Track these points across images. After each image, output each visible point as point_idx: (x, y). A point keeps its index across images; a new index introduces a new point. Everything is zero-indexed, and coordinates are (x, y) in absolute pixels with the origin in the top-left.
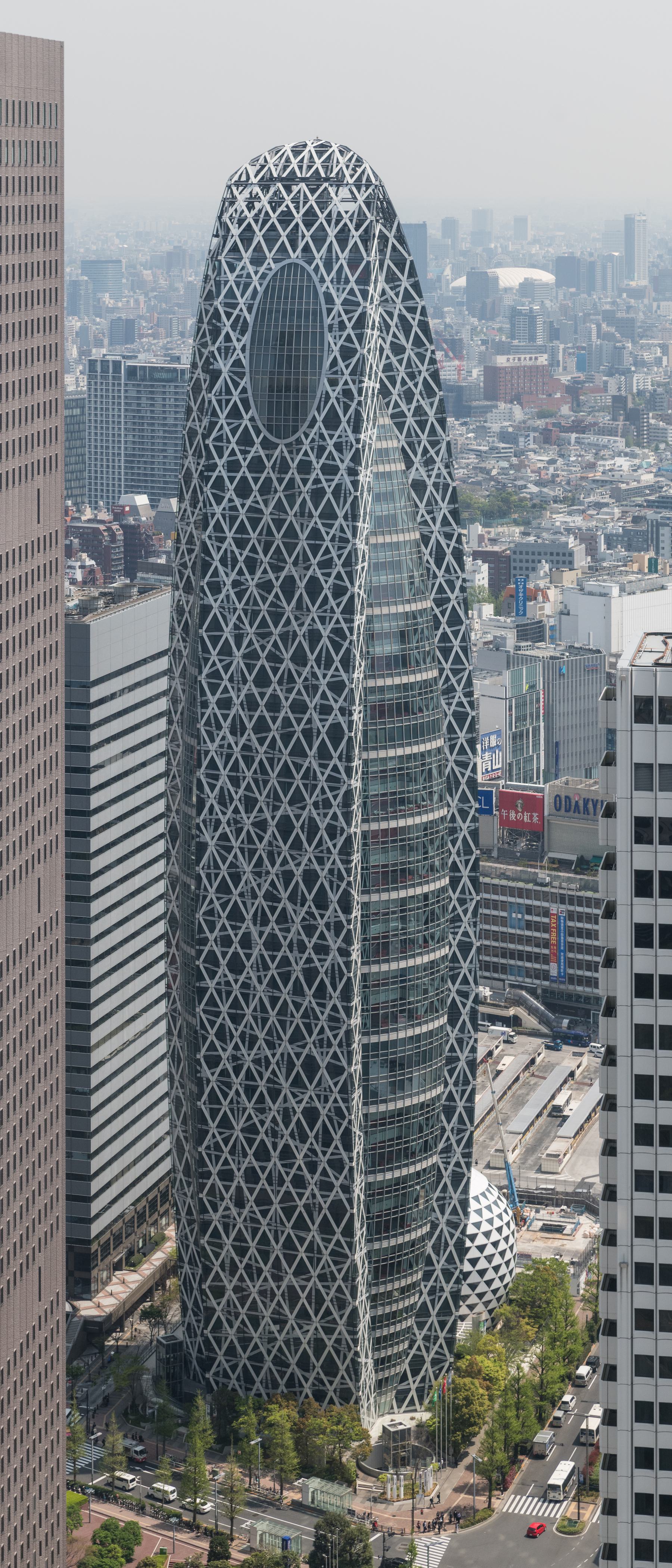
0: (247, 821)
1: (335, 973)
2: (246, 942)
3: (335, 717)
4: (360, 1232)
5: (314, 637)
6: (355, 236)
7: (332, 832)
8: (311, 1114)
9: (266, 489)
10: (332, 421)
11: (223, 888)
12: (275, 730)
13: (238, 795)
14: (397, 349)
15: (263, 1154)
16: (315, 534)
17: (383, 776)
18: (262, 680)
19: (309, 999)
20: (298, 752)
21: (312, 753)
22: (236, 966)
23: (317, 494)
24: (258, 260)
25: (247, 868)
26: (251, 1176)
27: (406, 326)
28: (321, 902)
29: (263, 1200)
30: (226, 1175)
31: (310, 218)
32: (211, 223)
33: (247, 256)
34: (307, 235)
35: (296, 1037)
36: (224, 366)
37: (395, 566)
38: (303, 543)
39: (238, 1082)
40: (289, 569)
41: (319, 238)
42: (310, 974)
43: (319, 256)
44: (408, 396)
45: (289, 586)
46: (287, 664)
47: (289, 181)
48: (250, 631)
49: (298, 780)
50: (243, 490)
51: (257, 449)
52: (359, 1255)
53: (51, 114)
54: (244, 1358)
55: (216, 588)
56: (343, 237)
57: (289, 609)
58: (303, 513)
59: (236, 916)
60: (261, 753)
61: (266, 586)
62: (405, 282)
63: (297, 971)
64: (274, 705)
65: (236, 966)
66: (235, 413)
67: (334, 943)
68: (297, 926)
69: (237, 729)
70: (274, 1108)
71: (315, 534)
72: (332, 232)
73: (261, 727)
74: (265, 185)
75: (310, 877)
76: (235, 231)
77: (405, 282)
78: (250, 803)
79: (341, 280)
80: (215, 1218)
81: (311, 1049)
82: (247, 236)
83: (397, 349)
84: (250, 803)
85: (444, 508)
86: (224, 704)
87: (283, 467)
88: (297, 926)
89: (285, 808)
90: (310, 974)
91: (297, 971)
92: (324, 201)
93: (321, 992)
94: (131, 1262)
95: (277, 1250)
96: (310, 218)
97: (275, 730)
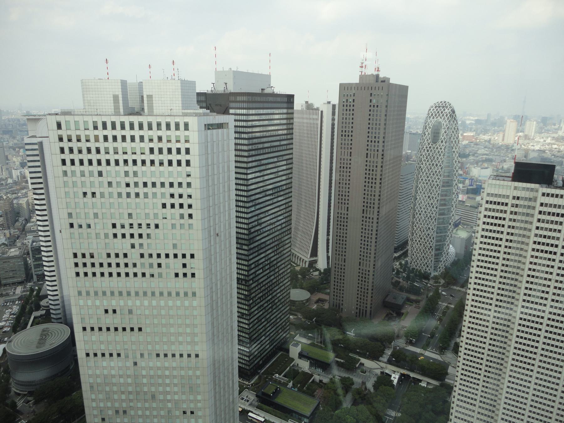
0: (424, 196)
1: (434, 217)
2: (422, 211)
3: (438, 183)
4: (434, 250)
5: (436, 172)
6: (449, 115)
7: (436, 198)
8: (429, 235)
9: (431, 151)
10: (442, 142)
11: (419, 204)
12: (429, 184)
13: (423, 192)
14: (453, 132)
15: (421, 239)
16: (438, 158)
17: (444, 191)
18: (428, 177)
19: (430, 220)
20: (432, 187)
21: (434, 187)
22: (420, 214)
23: (439, 152)
24: (433, 118)
25: (423, 202)
26: (419, 241)
27: (455, 129)
28: (433, 207)
29: (421, 244)
30: (416, 241)
31: (442, 112)
32: (427, 112)
33: (432, 118)
34: (441, 115)
35: (428, 224)
36: (427, 133)
37: (449, 163)
38: (436, 159)
39: (419, 229)
40: (433, 162)
41: (443, 115)
42: (430, 217)
43: (443, 118)
44: (454, 139)
45: (433, 165)
46: (432, 175)
47: (439, 107)
48: (427, 170)
49: (431, 191)
50: (428, 151)
51: (430, 145)
52: (433, 253)
53: (405, 96)
54: (416, 263)
55: (422, 164)
56: (447, 115)
57: (433, 168)
58: (436, 154)
59: (421, 208)
60: (427, 187)
61: (430, 164)
63: (429, 216)
64: (429, 181)
65: (420, 214)
66: (428, 140)
67: (434, 213)
68: (429, 210)
69: (423, 183)
70: (423, 233)
71: (438, 158)
72: (445, 115)
73: (427, 183)
74: (436, 107)
75: (432, 204)
76: (430, 114)
77: (455, 122)
78: (424, 193)
79: (445, 121)
80: (414, 246)
81: (429, 226)
82: (432, 115)
83: (453, 132)
84: (424, 193)
85: (457, 155)
86: (422, 180)
87: (434, 148)
88: (429, 210)
89: (429, 194)
90: (430, 217)
91: (429, 216)
92: (444, 110)
93: (432, 219)
94: (401, 250)
95: (422, 251)
96: (442, 112)
97: (429, 184)
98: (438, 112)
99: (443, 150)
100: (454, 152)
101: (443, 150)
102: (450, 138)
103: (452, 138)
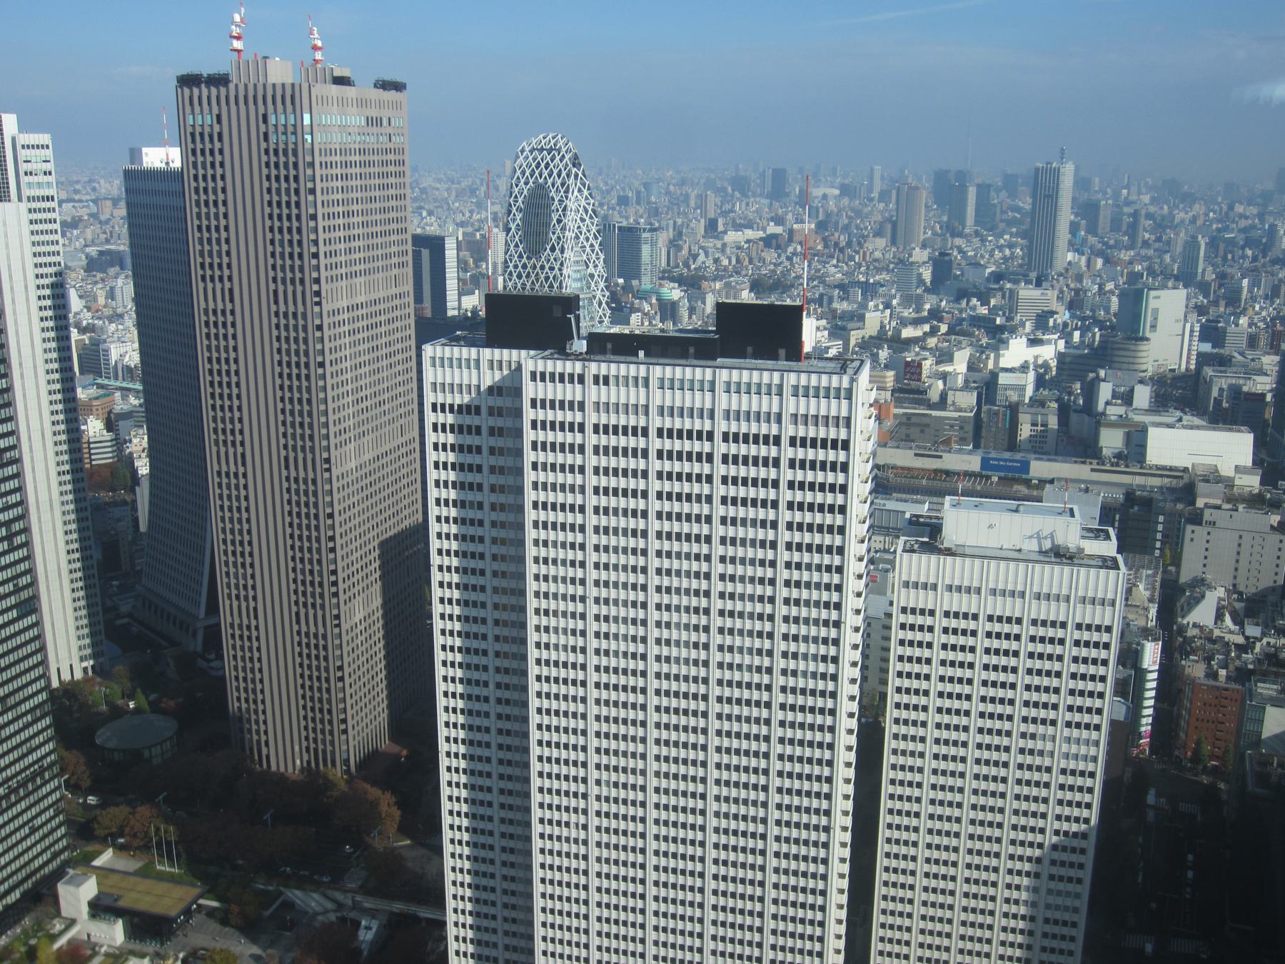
9: (528, 276)
10: (553, 249)
14: (583, 220)
23: (547, 278)
31: (547, 166)
34: (546, 173)
36: (513, 226)
50: (519, 276)
62: (586, 192)
83: (583, 220)
96: (547, 166)
98: (538, 166)
99: (556, 271)
100: (592, 276)
101: (556, 271)
102: (577, 237)
103: (582, 238)
